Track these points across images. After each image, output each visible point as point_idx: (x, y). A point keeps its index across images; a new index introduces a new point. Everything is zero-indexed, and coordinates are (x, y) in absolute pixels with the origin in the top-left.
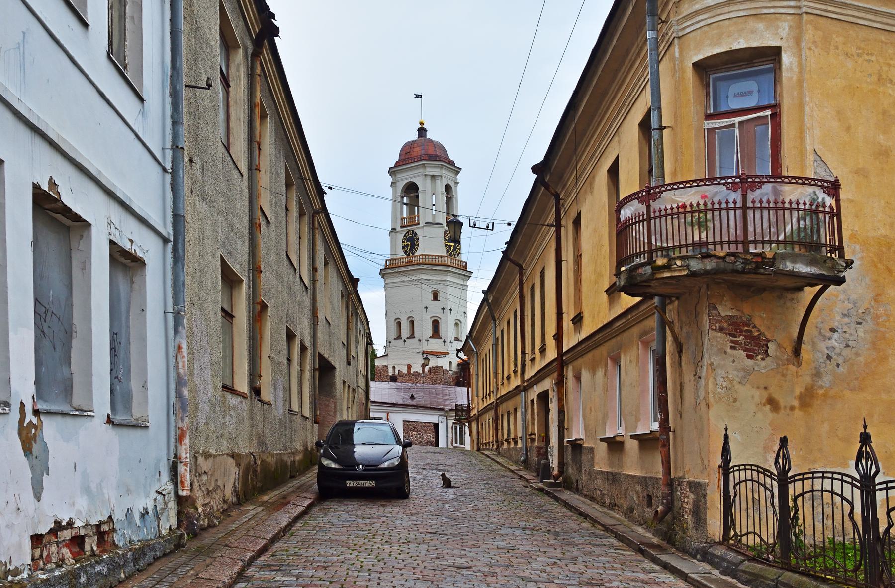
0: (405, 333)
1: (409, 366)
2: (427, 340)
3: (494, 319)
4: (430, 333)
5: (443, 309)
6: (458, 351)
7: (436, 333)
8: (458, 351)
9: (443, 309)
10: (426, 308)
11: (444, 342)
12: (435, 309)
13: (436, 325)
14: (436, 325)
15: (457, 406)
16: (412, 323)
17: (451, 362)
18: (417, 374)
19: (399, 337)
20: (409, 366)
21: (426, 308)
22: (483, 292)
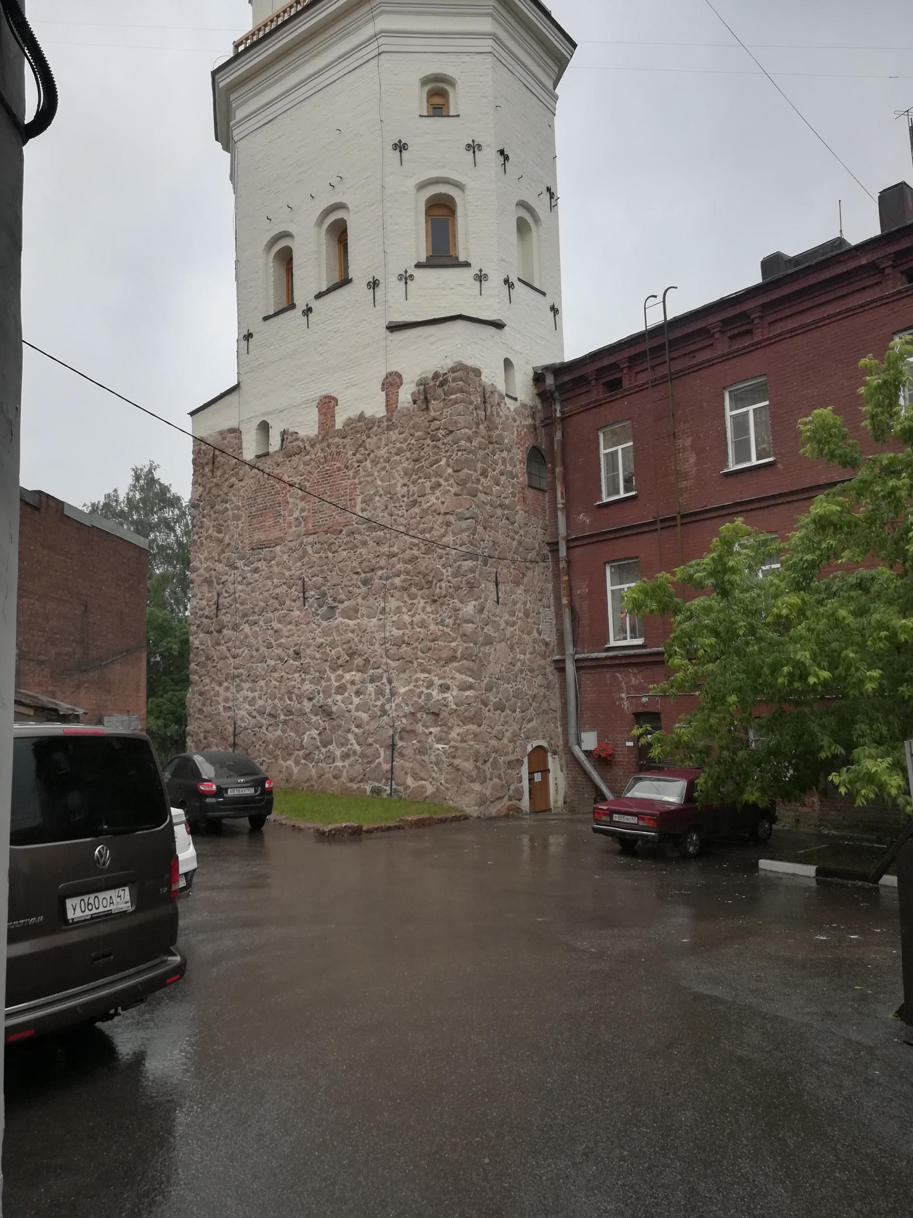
0: (311, 274)
1: (327, 405)
2: (406, 278)
4: (414, 242)
5: (473, 147)
7: (442, 254)
9: (473, 147)
10: (401, 147)
11: (481, 278)
12: (438, 149)
13: (441, 211)
14: (441, 211)
16: (339, 234)
18: (362, 426)
20: (327, 405)
21: (401, 147)
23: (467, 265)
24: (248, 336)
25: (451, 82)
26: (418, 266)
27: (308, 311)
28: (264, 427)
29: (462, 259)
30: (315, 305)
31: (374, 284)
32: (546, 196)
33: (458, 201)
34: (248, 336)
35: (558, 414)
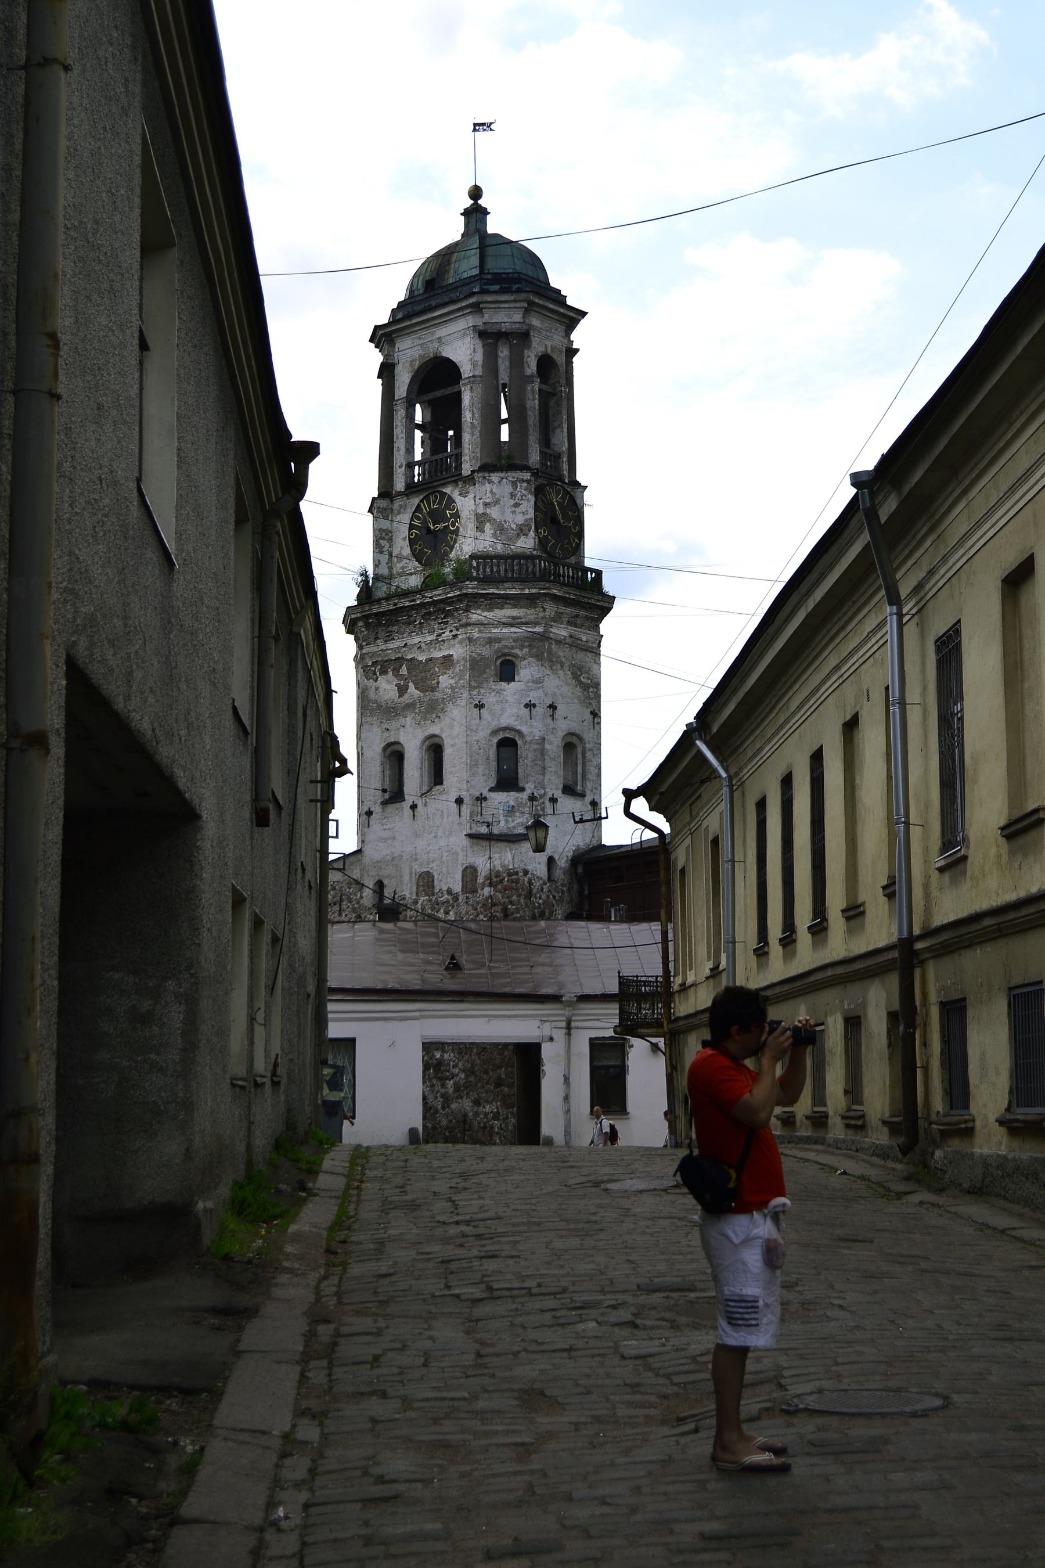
3: (894, 599)
5: (530, 706)
6: (629, 795)
7: (507, 781)
8: (629, 795)
9: (530, 706)
15: (623, 982)
17: (551, 861)
19: (394, 795)
22: (857, 480)
23: (523, 789)
24: (369, 813)
25: (516, 656)
26: (491, 790)
27: (414, 807)
28: (380, 885)
29: (521, 785)
30: (419, 803)
31: (459, 801)
32: (590, 717)
33: (519, 742)
34: (369, 813)
35: (586, 892)
